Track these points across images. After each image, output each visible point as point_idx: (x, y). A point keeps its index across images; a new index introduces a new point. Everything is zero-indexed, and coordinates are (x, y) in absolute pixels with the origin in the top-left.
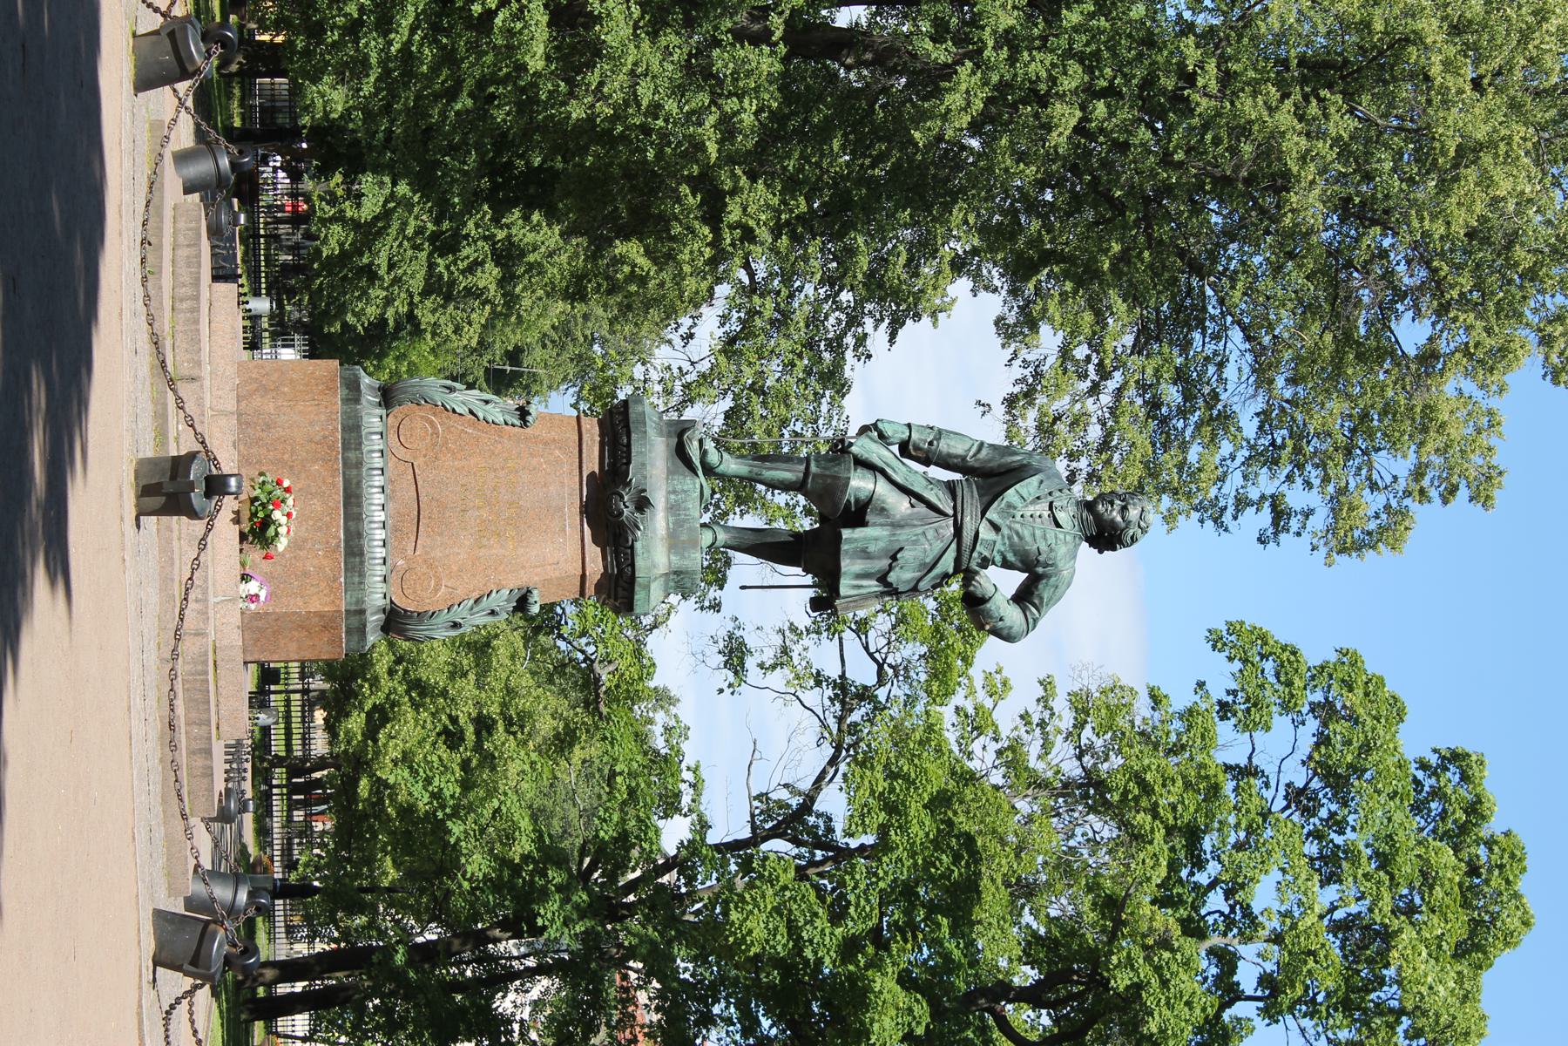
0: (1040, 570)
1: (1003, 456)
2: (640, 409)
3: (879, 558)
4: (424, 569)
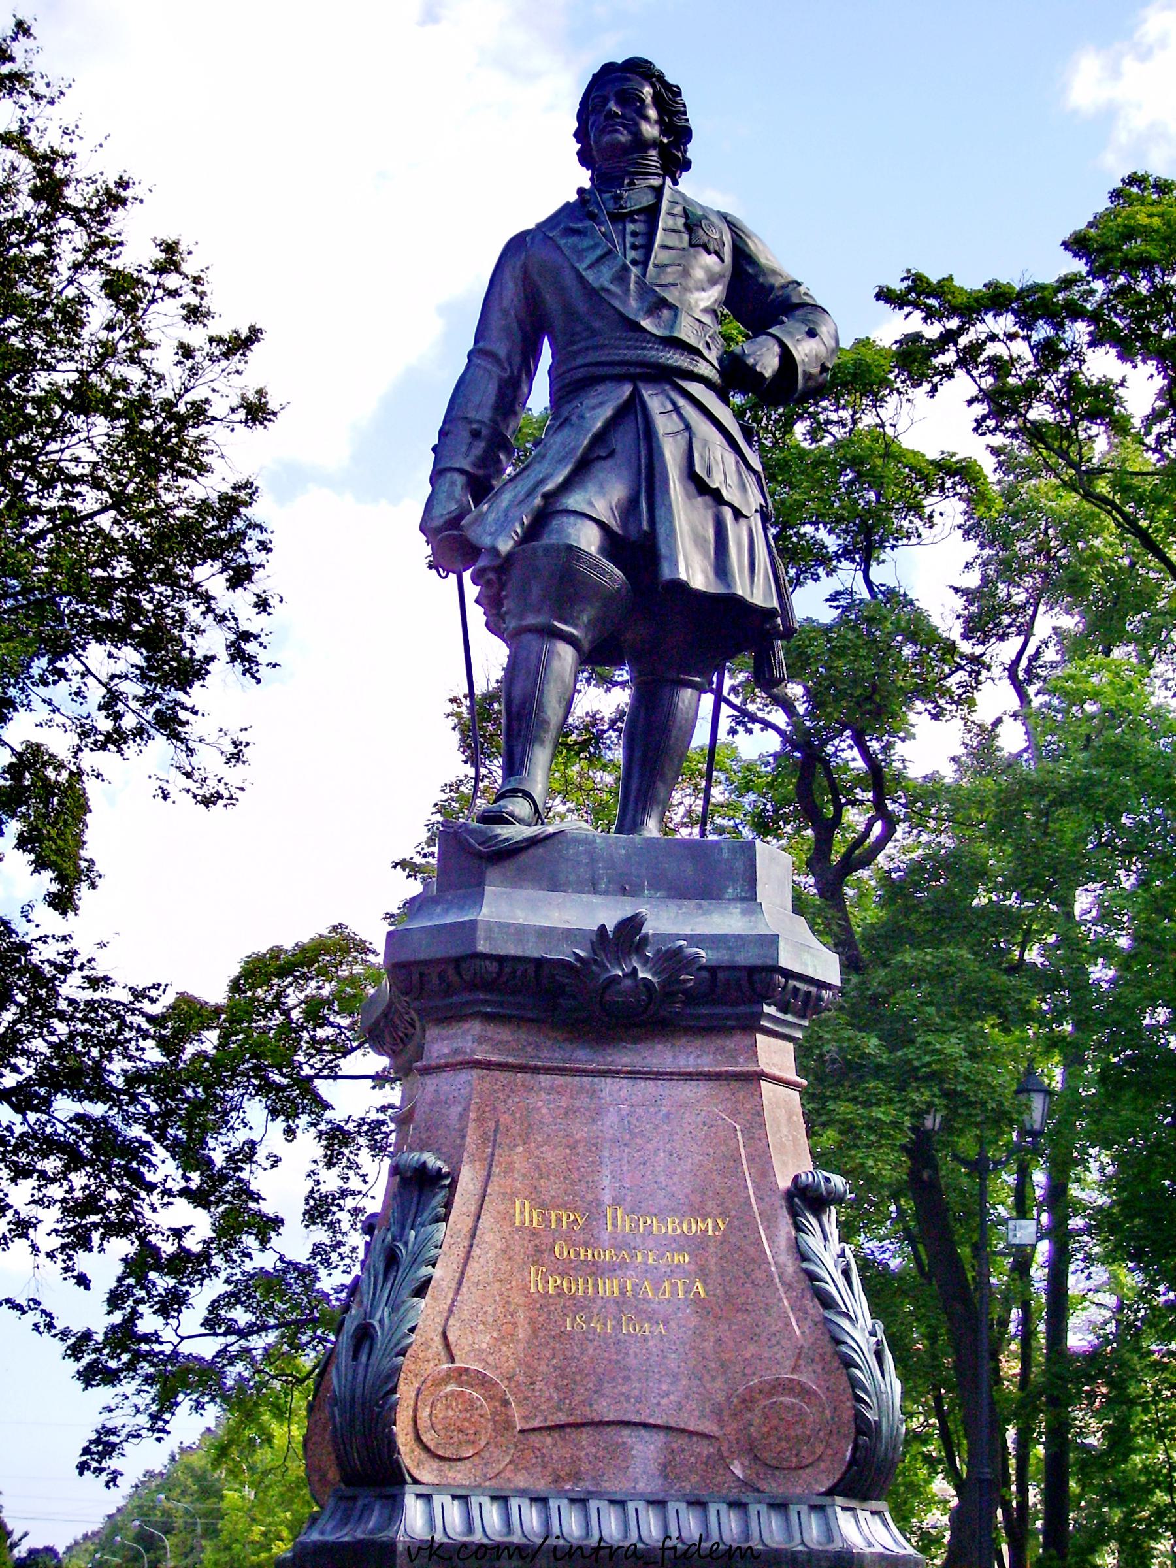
4: (756, 1417)
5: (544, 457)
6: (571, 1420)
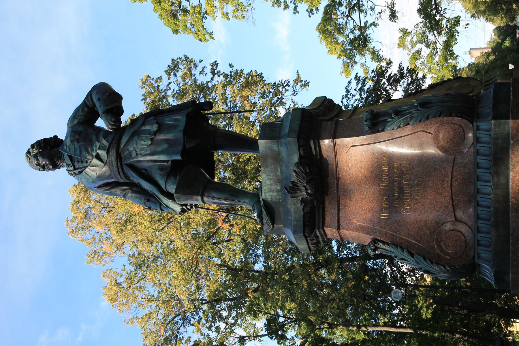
6: (451, 203)
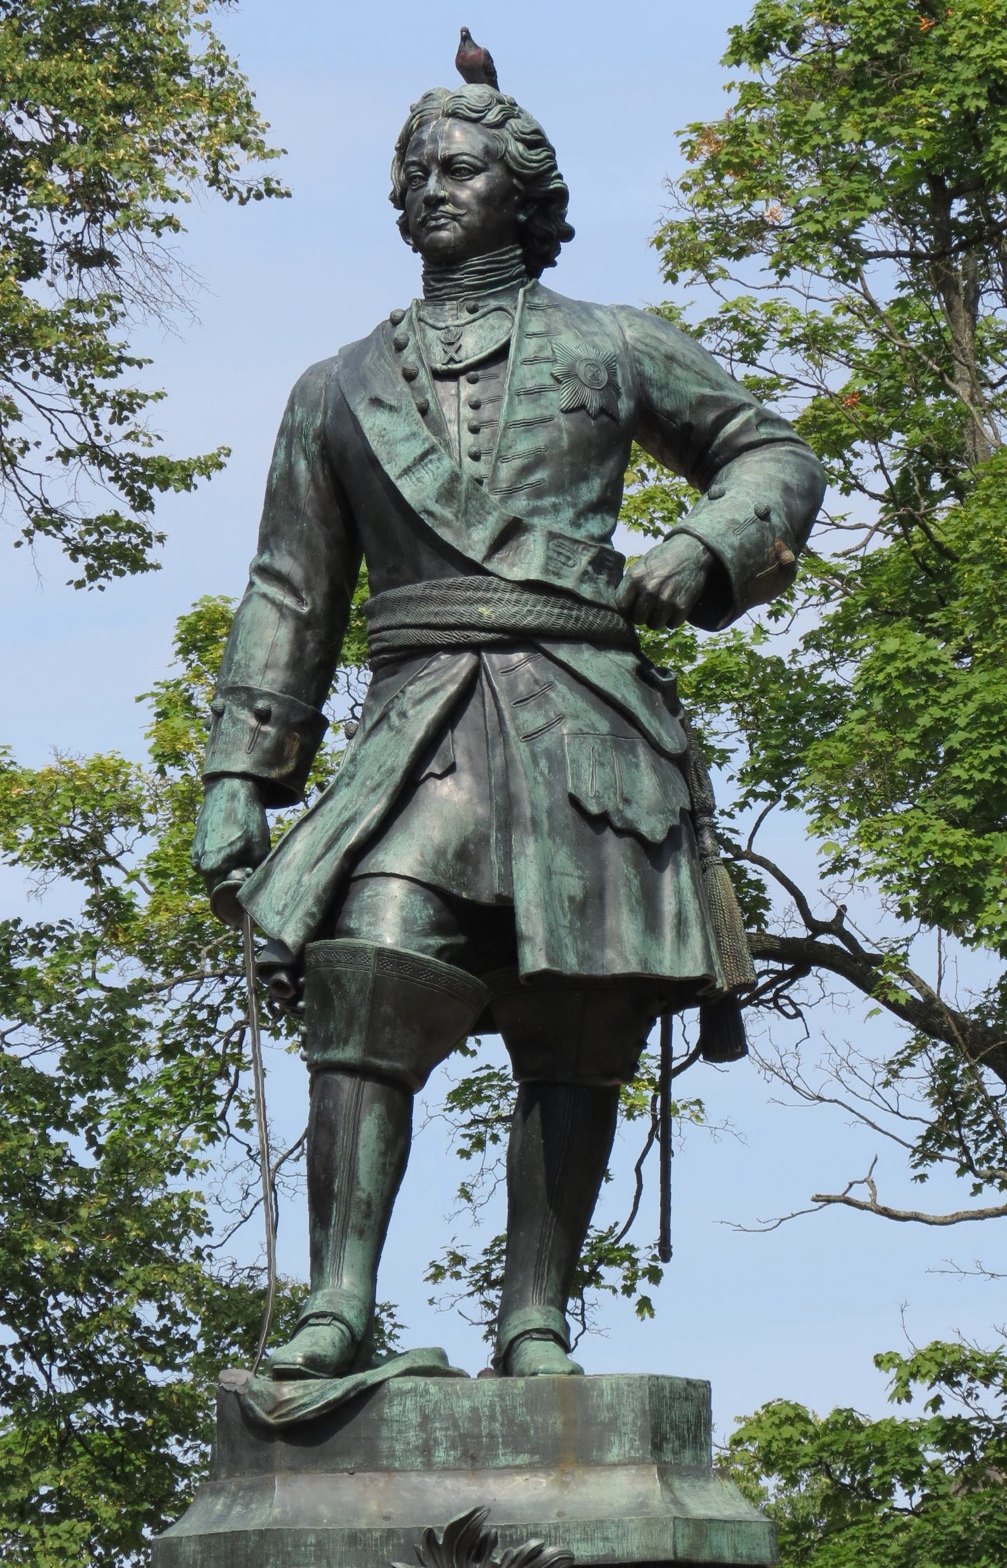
0: (624, 406)
1: (297, 512)
2: (190, 1549)
3: (600, 865)
5: (352, 777)
